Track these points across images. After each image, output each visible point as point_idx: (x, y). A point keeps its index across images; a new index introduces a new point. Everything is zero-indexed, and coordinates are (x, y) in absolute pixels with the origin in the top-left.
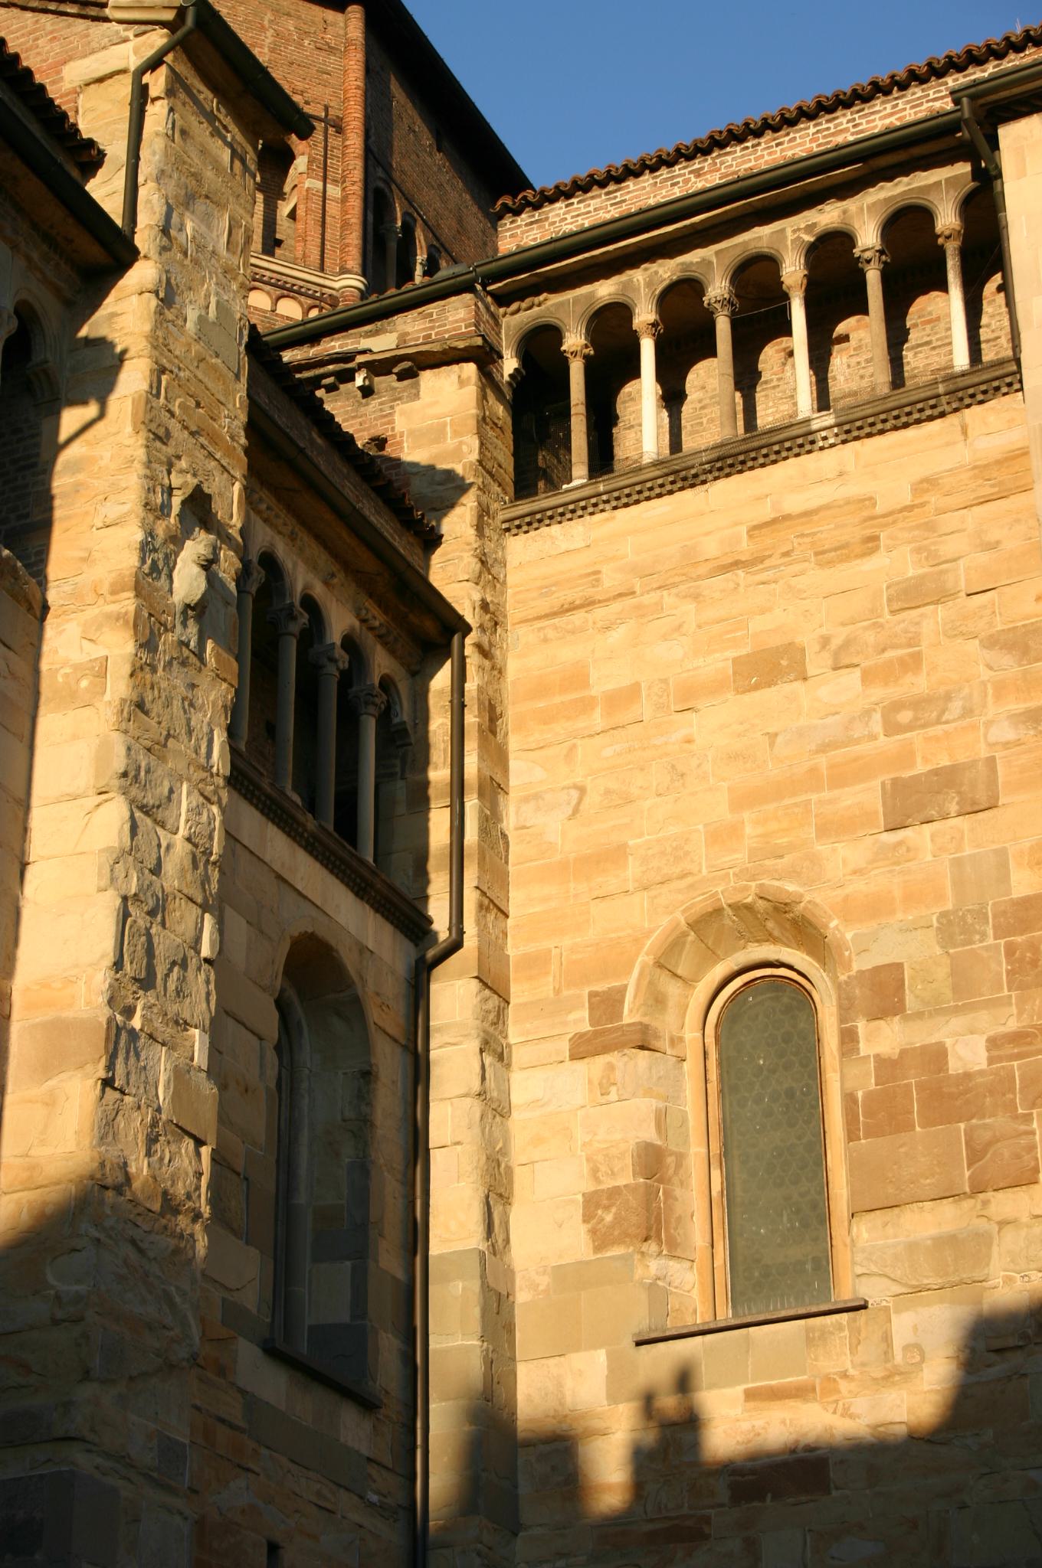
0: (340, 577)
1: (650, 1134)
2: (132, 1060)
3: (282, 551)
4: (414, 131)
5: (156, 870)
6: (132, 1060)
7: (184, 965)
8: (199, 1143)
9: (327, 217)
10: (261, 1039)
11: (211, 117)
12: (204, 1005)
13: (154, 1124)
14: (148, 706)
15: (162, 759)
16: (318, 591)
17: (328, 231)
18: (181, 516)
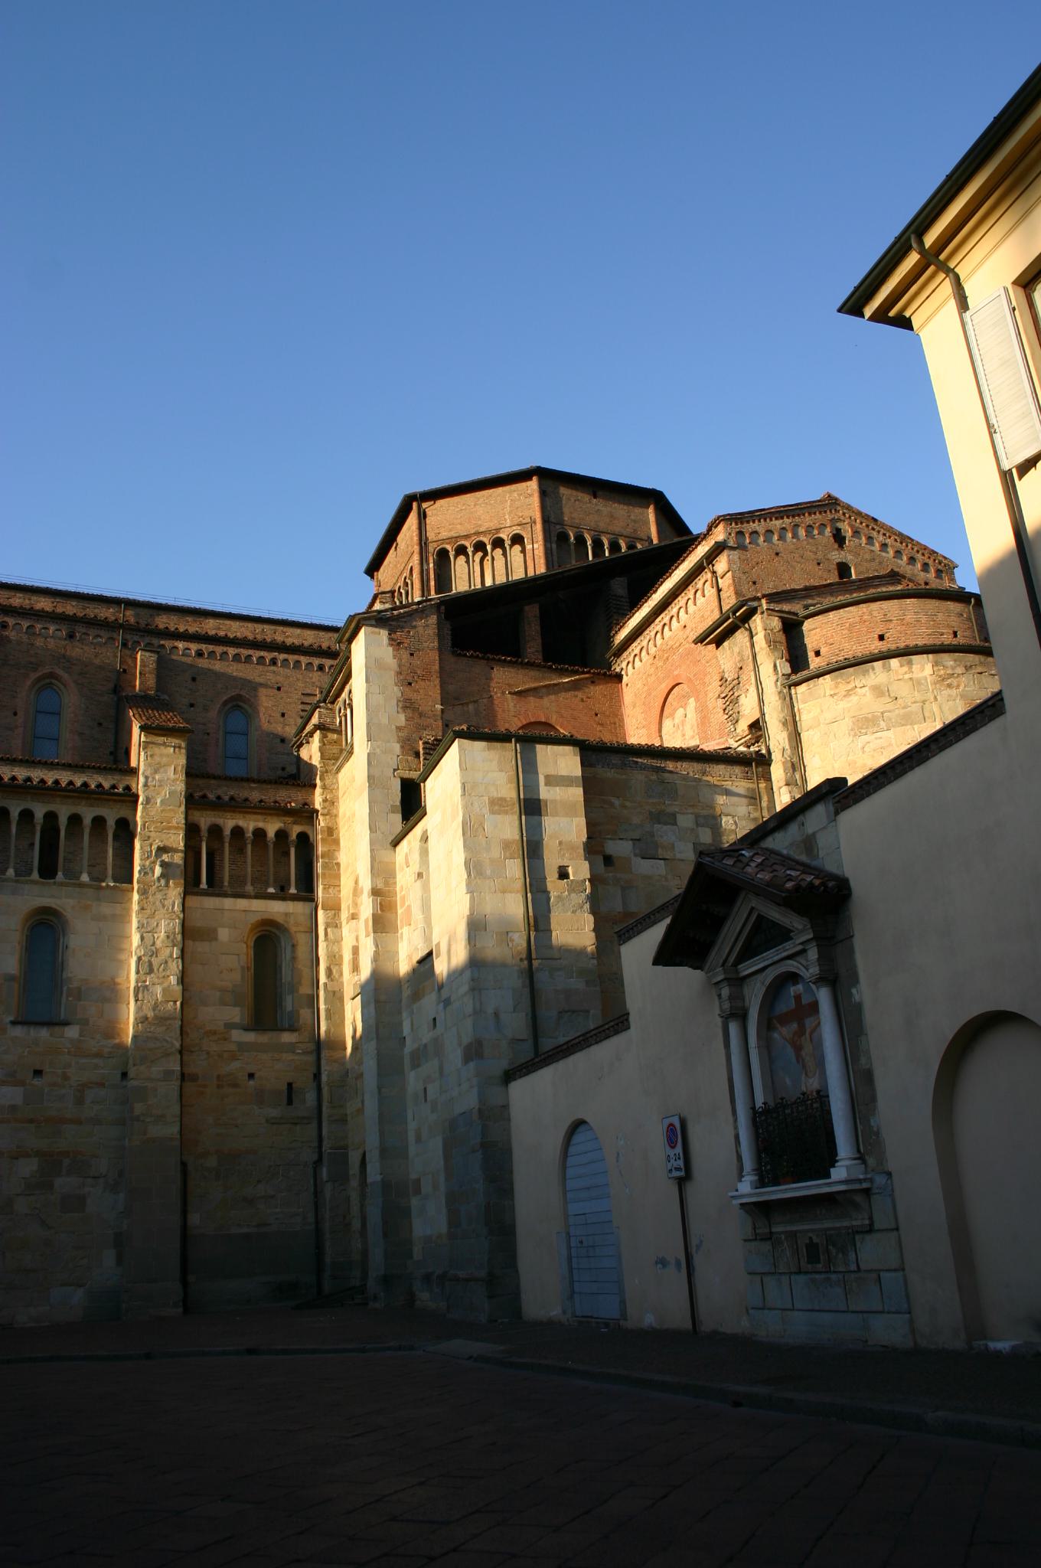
1: (355, 943)
3: (241, 823)
4: (578, 500)
5: (154, 944)
6: (146, 992)
7: (166, 962)
8: (175, 1002)
11: (164, 744)
12: (176, 969)
14: (145, 908)
16: (261, 825)
18: (156, 855)
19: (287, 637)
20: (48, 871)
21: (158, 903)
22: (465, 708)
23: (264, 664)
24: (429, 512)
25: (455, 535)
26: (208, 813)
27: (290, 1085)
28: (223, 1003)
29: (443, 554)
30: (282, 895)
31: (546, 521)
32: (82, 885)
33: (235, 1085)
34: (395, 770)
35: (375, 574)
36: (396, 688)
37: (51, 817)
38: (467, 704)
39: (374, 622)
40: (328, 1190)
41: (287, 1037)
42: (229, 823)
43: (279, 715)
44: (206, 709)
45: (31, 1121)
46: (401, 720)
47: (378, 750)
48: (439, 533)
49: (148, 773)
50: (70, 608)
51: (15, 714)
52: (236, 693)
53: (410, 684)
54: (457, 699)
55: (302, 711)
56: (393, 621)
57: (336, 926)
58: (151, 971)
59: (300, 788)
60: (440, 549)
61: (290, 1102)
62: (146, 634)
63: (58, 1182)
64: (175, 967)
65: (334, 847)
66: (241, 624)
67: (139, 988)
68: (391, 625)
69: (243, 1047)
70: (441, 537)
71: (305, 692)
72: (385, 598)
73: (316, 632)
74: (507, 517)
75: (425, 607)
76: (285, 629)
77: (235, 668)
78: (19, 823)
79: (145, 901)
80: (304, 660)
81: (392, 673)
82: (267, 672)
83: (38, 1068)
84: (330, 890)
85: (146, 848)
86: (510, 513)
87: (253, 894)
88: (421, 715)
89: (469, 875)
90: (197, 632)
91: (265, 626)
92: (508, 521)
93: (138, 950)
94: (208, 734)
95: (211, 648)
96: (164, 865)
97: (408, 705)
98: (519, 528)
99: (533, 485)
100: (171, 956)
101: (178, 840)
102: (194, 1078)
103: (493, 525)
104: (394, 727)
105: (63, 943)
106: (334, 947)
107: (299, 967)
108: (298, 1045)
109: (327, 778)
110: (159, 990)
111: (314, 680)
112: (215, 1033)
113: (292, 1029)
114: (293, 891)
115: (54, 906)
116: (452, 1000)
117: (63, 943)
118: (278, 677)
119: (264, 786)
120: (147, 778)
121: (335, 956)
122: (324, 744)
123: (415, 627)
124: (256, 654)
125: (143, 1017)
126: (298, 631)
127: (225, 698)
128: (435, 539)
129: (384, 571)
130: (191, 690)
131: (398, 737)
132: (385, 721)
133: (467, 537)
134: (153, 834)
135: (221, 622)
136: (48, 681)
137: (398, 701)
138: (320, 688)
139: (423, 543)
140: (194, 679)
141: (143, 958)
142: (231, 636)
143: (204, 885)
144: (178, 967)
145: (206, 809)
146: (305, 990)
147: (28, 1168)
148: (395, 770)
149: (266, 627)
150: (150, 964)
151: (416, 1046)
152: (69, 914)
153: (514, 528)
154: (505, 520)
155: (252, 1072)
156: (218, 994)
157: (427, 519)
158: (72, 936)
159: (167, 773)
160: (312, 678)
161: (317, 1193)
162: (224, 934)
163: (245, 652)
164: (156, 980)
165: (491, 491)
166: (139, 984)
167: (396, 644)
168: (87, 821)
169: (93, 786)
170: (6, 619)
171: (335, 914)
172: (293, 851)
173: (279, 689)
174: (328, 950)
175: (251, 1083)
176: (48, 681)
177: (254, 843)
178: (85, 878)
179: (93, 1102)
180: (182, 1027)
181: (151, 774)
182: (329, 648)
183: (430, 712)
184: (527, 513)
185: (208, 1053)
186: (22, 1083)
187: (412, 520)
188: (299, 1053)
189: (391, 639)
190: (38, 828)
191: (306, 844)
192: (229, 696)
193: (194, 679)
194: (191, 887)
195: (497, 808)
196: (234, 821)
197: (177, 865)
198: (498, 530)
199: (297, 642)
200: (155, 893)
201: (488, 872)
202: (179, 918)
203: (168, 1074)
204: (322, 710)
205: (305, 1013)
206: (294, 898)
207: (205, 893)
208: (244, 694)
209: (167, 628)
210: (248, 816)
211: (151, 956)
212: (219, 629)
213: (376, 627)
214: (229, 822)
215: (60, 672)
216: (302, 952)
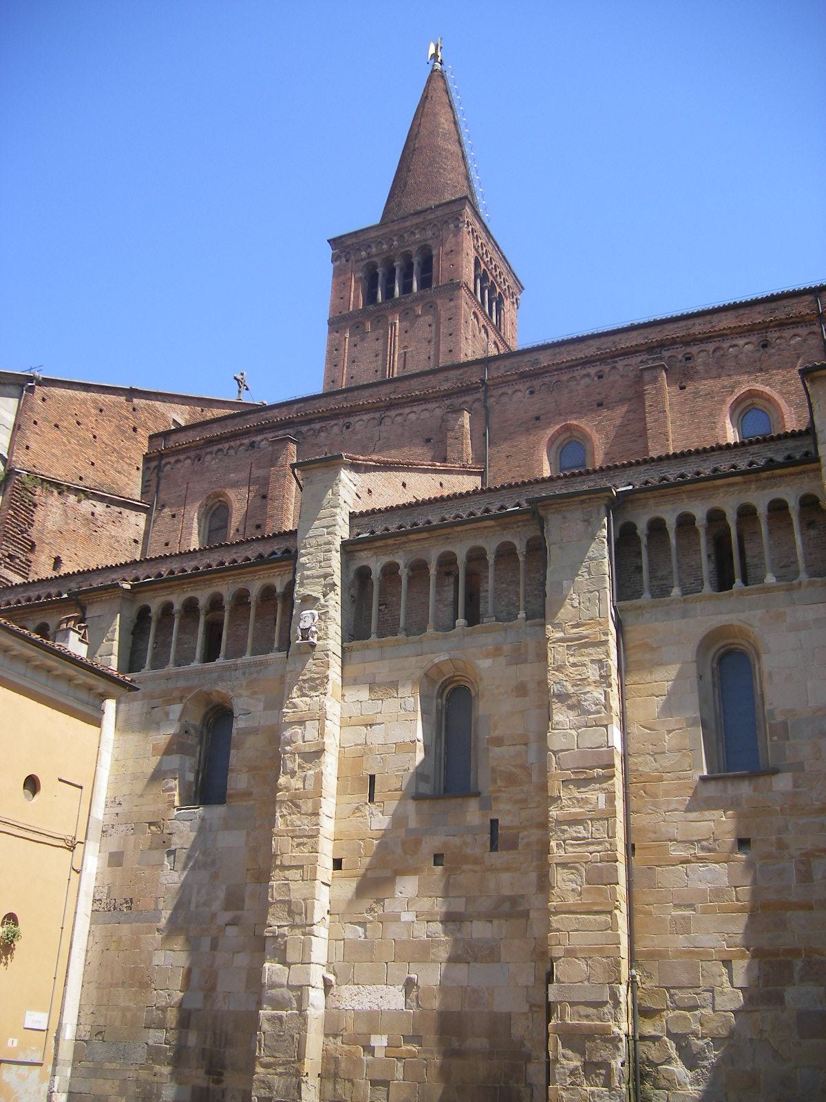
20: (723, 582)
32: (768, 589)
37: (716, 517)
50: (757, 316)
63: (790, 993)
115: (736, 623)
136: (748, 402)
168: (762, 510)
170: (689, 350)
176: (748, 402)
178: (770, 579)
190: (702, 531)
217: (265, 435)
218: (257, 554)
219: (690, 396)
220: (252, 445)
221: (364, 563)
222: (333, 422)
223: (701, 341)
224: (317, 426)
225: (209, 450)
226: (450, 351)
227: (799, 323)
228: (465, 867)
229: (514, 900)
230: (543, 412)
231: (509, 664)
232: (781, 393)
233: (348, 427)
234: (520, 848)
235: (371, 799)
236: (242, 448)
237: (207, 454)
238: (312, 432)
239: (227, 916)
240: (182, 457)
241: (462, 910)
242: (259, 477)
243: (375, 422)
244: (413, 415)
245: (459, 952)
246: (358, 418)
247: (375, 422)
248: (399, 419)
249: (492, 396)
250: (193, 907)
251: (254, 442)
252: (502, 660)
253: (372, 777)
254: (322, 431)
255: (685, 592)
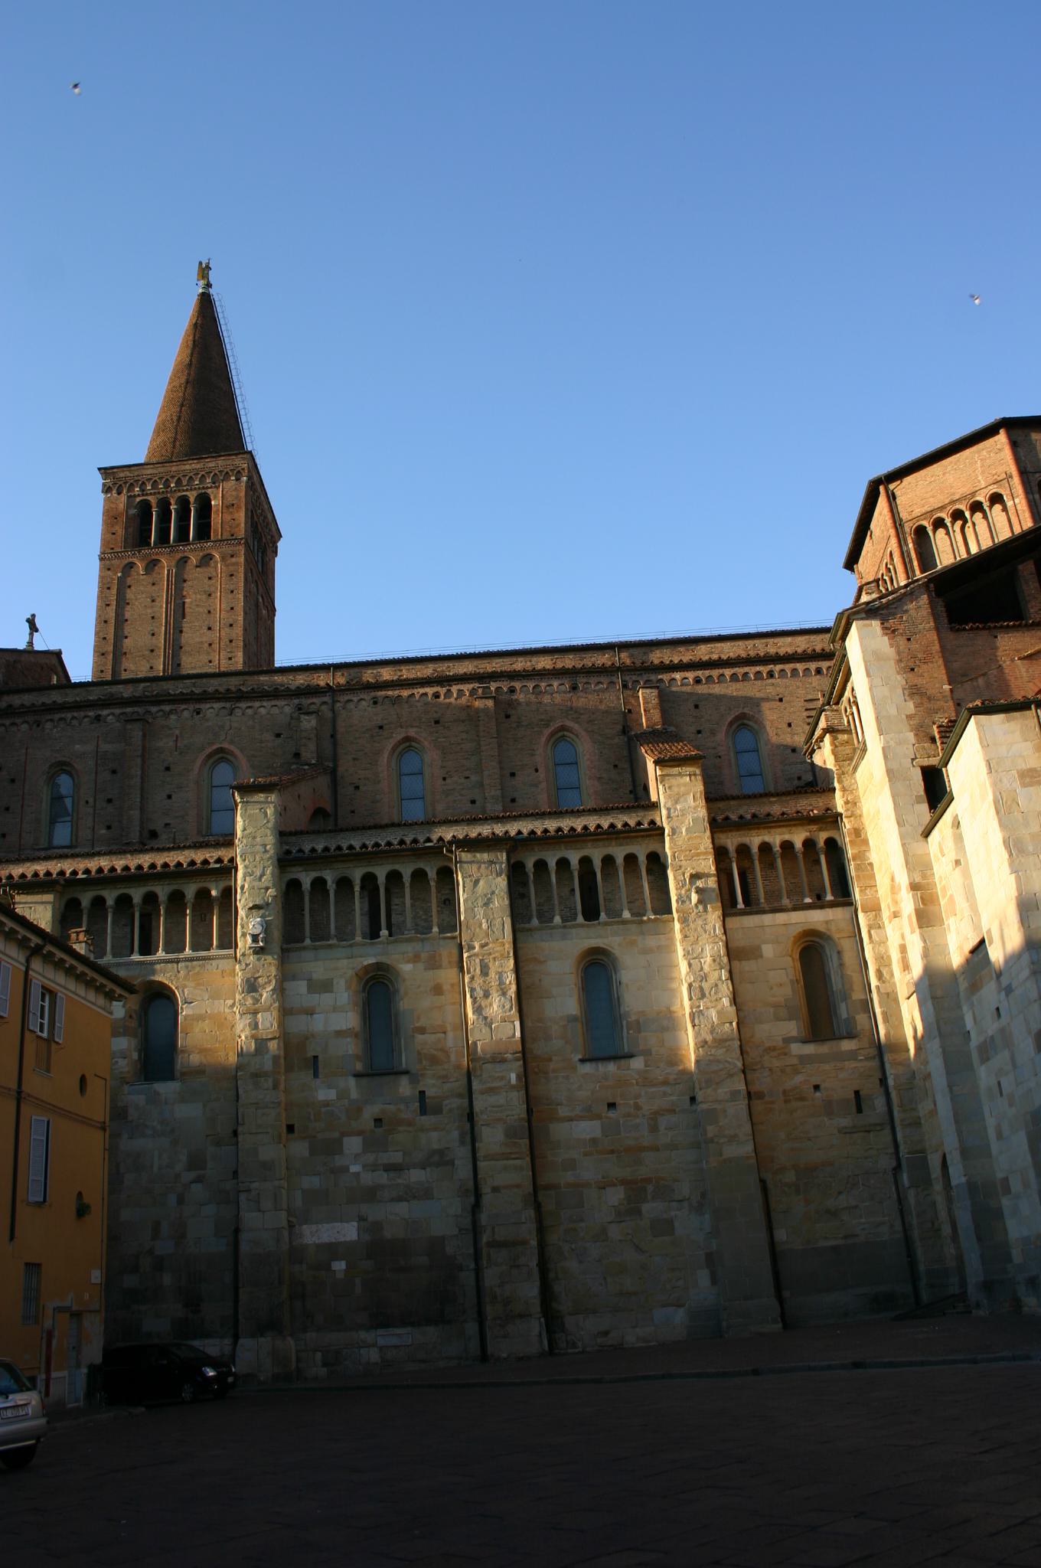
0: (794, 829)
2: (701, 1017)
3: (767, 839)
5: (702, 969)
6: (701, 1017)
7: (716, 985)
8: (731, 1023)
9: (1019, 512)
10: (785, 969)
11: (680, 775)
12: (727, 991)
13: (712, 1027)
15: (698, 943)
16: (787, 837)
17: (1020, 517)
18: (690, 883)
19: (780, 647)
20: (591, 913)
21: (699, 929)
22: (975, 683)
23: (762, 679)
24: (897, 493)
25: (929, 509)
26: (734, 834)
27: (857, 1093)
28: (778, 1019)
29: (921, 532)
30: (819, 903)
31: (1023, 473)
32: (625, 922)
33: (802, 1099)
34: (913, 760)
35: (855, 566)
36: (899, 677)
37: (586, 861)
38: (976, 678)
39: (864, 615)
40: (911, 1197)
41: (847, 1045)
42: (755, 840)
43: (785, 726)
44: (713, 733)
45: (612, 1152)
46: (910, 707)
47: (892, 743)
48: (912, 511)
49: (669, 805)
50: (569, 662)
51: (537, 770)
52: (740, 712)
53: (913, 670)
54: (964, 675)
55: (808, 717)
56: (883, 609)
57: (880, 927)
58: (703, 996)
59: (820, 795)
60: (916, 528)
61: (859, 1110)
62: (643, 672)
63: (645, 1208)
64: (726, 989)
65: (864, 848)
66: (732, 644)
67: (694, 1014)
68: (881, 614)
69: (804, 1059)
70: (915, 514)
71: (807, 698)
72: (870, 588)
73: (807, 637)
74: (980, 478)
75: (913, 588)
76: (776, 640)
77: (734, 688)
78: (557, 872)
79: (686, 929)
80: (800, 667)
81: (892, 663)
82: (766, 685)
83: (611, 1101)
84: (867, 891)
85: (679, 877)
86: (983, 473)
87: (790, 906)
88: (929, 699)
89: (1011, 855)
90: (691, 660)
91: (755, 641)
92: (982, 482)
93: (688, 977)
94: (720, 757)
95: (707, 673)
96: (699, 891)
97: (914, 691)
98: (995, 486)
99: (1002, 438)
100: (720, 979)
101: (709, 865)
102: (760, 1095)
103: (966, 490)
104: (904, 717)
105: (616, 979)
106: (881, 949)
107: (849, 973)
108: (858, 1051)
109: (845, 779)
110: (713, 1013)
111: (814, 685)
112: (774, 1049)
113: (851, 1036)
114: (829, 897)
116: (1013, 987)
117: (616, 979)
118: (778, 689)
119: (784, 798)
120: (669, 809)
121: (882, 958)
122: (836, 746)
123: (906, 611)
124: (752, 670)
125: (702, 1042)
126: (789, 639)
127: (730, 719)
128: (910, 518)
129: (863, 562)
130: (696, 717)
131: (910, 725)
132: (893, 711)
133: (942, 508)
134: (683, 863)
135: (712, 646)
136: (560, 734)
137: (904, 689)
138: (822, 691)
139: (897, 523)
140: (696, 707)
141: (694, 984)
142: (724, 657)
143: (741, 905)
144: (728, 989)
145: (731, 831)
146: (857, 995)
147: (616, 1196)
148: (913, 760)
149: (757, 642)
150: (701, 989)
151: (982, 1039)
152: (616, 951)
153: (991, 487)
154: (979, 481)
155: (818, 1083)
156: (772, 1010)
157: (897, 500)
158: (623, 972)
159: (687, 801)
160: (811, 683)
161: (900, 1201)
162: (768, 950)
163: (740, 671)
164: (709, 1004)
165: (958, 455)
166: (694, 1010)
167: (890, 632)
168: (620, 860)
169: (619, 826)
170: (512, 684)
171: (876, 915)
172: (823, 858)
173: (781, 700)
174: (874, 953)
175: (818, 1094)
176: (560, 734)
177: (783, 856)
178: (626, 915)
179: (666, 1129)
180: (741, 1046)
181: (673, 805)
182: (823, 650)
183: (939, 695)
184: (1004, 468)
185: (770, 1070)
186: (598, 1117)
187: (882, 504)
188: (861, 1060)
189: (884, 628)
190: (576, 874)
191: (834, 849)
192: (733, 716)
193: (696, 707)
194: (729, 908)
195: (1028, 780)
196: (760, 838)
197: (712, 890)
198: (973, 494)
199: (790, 651)
200: (695, 920)
201: (1031, 848)
202: (722, 941)
203: (734, 1094)
204: (828, 713)
205: (861, 1019)
206: (832, 905)
207: (743, 913)
208: (748, 712)
209: (662, 662)
210: (773, 830)
211: (701, 981)
212: (712, 653)
213: (867, 619)
214: (755, 840)
215: (569, 724)
216: (849, 958)
217: (112, 711)
218: (189, 860)
219: (514, 725)
220: (98, 718)
221: (295, 876)
222: (183, 707)
223: (524, 677)
224: (167, 708)
225: (49, 717)
226: (232, 608)
227: (603, 672)
228: (401, 1129)
229: (441, 1153)
230: (385, 722)
231: (426, 969)
232: (586, 730)
233: (198, 713)
234: (444, 1112)
235: (316, 1075)
236: (86, 720)
237: (47, 721)
238: (161, 713)
239: (193, 1175)
240: (18, 721)
241: (401, 1161)
242: (107, 751)
243: (225, 712)
244: (262, 709)
245: (401, 1193)
246: (208, 706)
247: (225, 712)
248: (249, 711)
249: (339, 701)
250: (155, 1169)
251: (99, 715)
252: (420, 966)
253: (316, 1058)
254: (172, 713)
255: (564, 920)
